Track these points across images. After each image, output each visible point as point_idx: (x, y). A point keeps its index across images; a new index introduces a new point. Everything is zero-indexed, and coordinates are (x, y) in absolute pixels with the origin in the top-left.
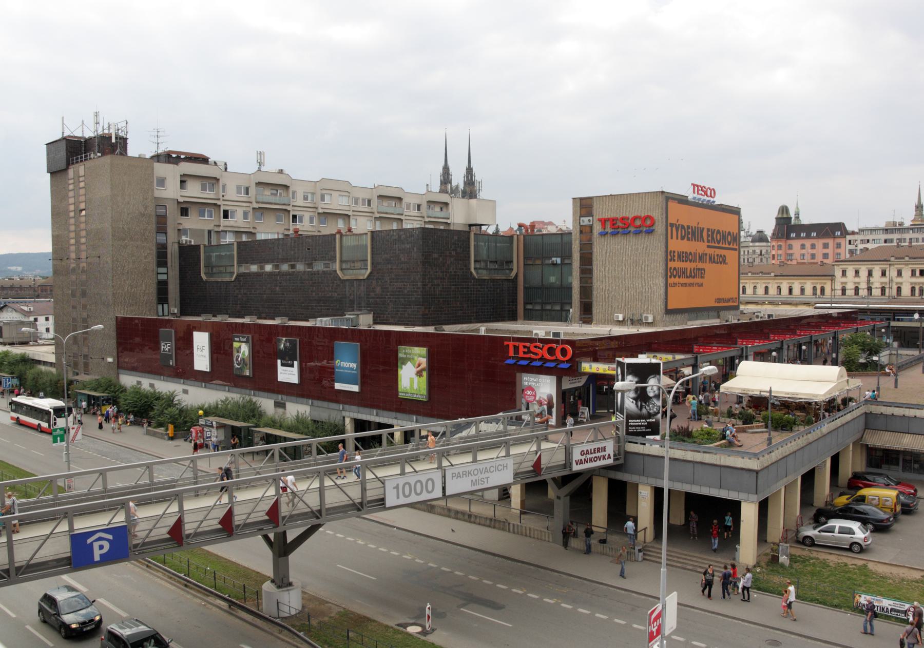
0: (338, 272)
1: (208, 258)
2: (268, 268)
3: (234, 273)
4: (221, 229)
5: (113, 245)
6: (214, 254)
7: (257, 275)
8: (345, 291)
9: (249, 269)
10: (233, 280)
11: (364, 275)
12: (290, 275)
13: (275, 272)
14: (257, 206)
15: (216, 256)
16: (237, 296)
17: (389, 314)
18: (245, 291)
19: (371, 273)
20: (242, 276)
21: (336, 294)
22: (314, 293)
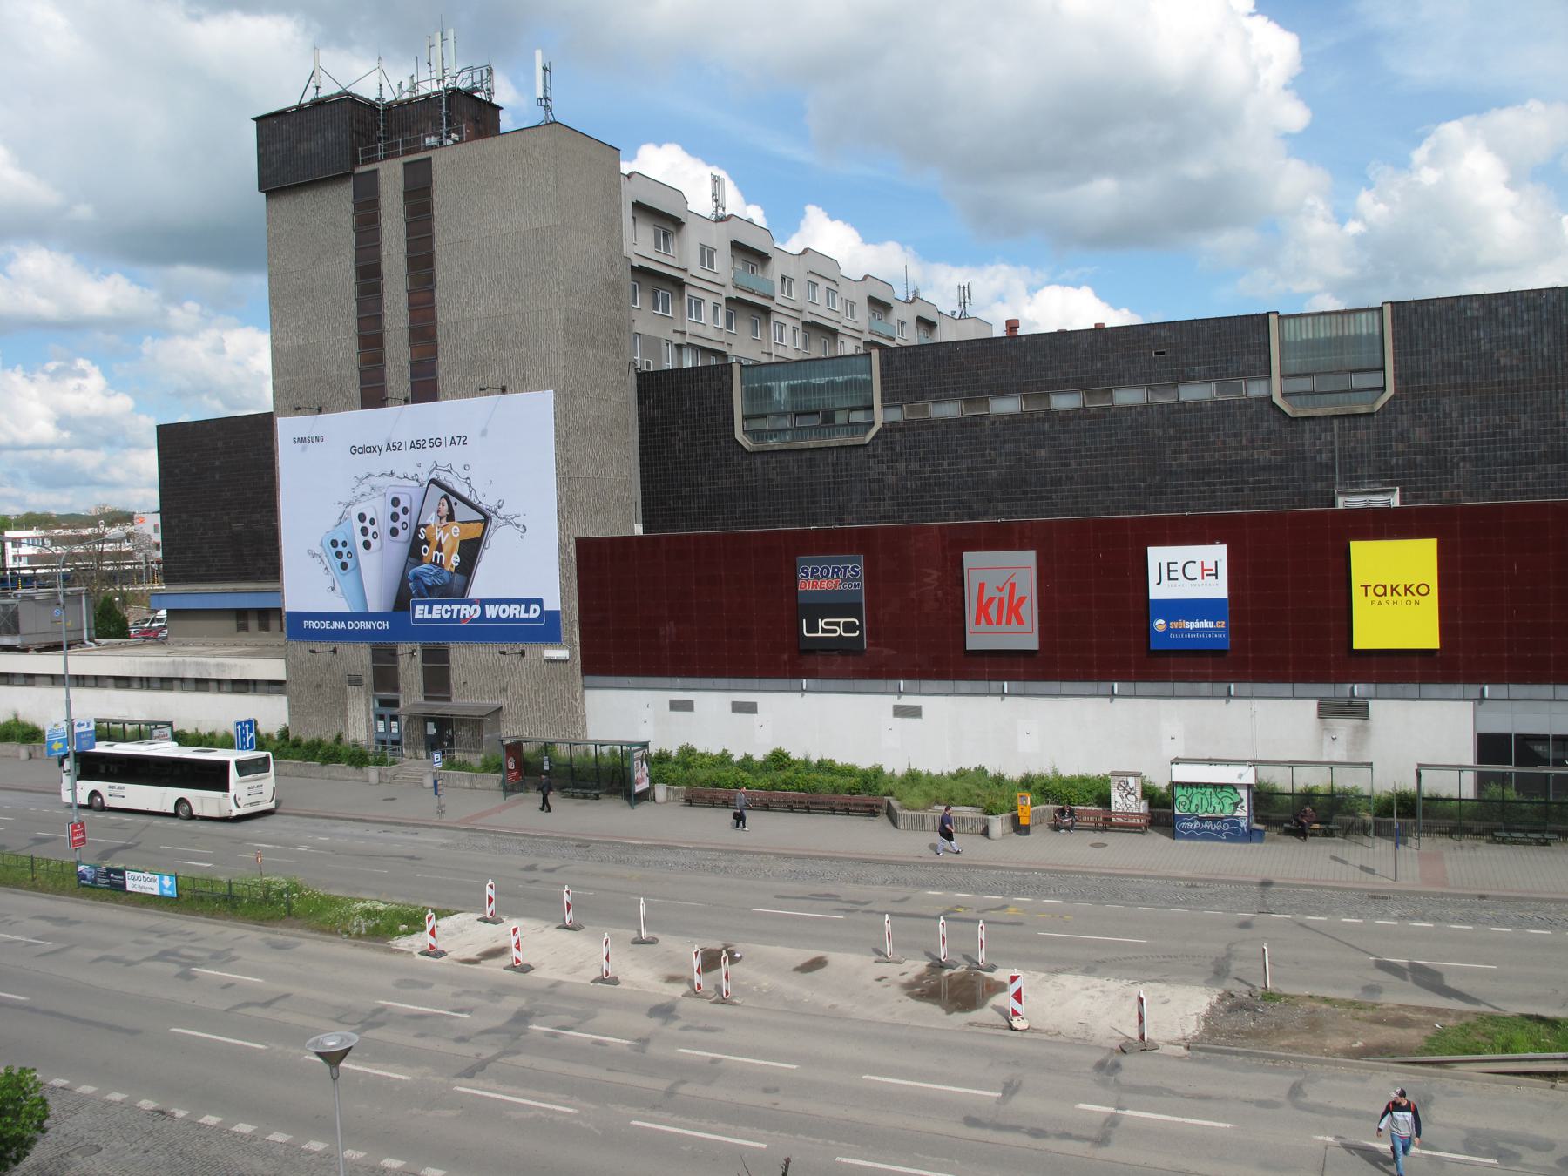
0: (1277, 400)
1: (759, 395)
2: (1006, 406)
3: (872, 424)
4: (688, 340)
5: (565, 353)
6: (783, 384)
7: (964, 425)
8: (1303, 445)
9: (926, 410)
10: (866, 443)
11: (1374, 402)
12: (1094, 416)
13: (1031, 414)
14: (734, 294)
15: (791, 388)
16: (879, 481)
17: (1458, 487)
18: (914, 466)
19: (1394, 397)
20: (900, 430)
21: (1267, 453)
22: (1074, 467)
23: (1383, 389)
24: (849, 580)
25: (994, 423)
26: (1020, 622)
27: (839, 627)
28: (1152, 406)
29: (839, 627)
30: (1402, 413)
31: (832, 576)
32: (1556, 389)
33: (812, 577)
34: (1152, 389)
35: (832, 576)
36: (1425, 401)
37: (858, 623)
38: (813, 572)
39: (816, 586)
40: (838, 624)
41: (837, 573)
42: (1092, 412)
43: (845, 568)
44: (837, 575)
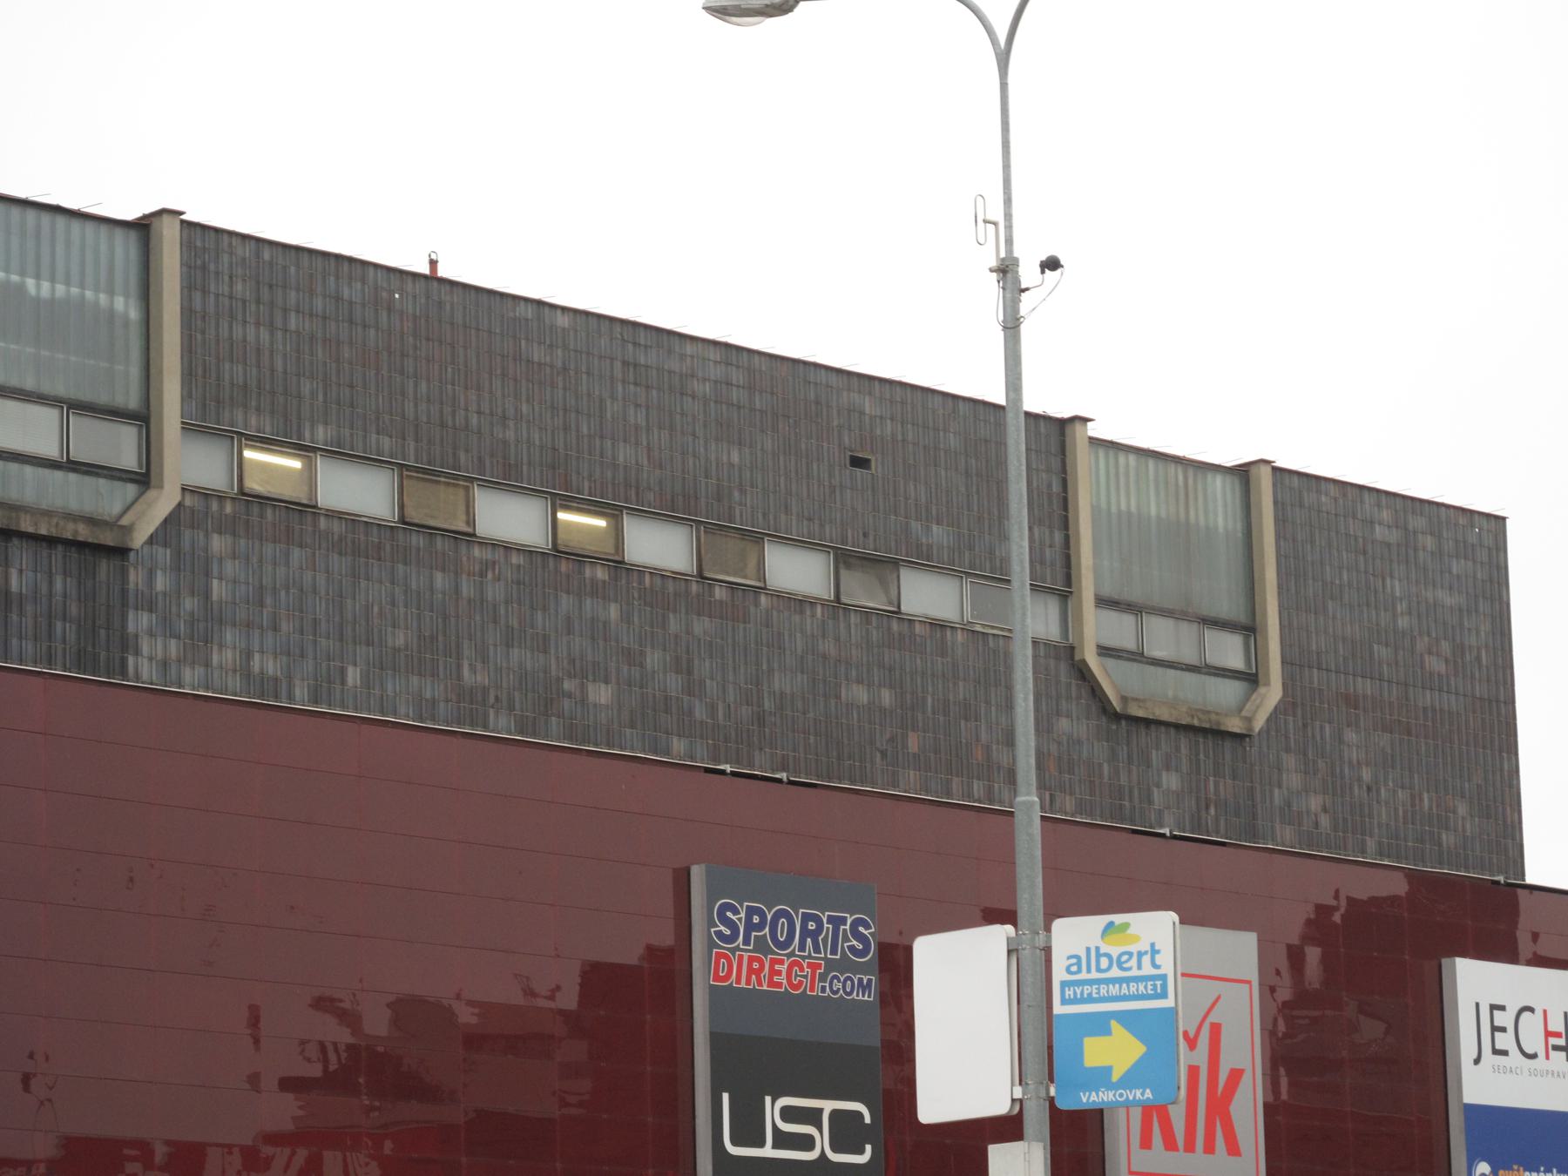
23: (1252, 678)
24: (844, 965)
25: (487, 566)
26: (1233, 1149)
27: (820, 1128)
28: (847, 609)
29: (820, 1128)
30: (1288, 750)
31: (802, 947)
32: (1501, 751)
33: (747, 942)
34: (845, 563)
35: (802, 947)
36: (1322, 728)
37: (868, 1120)
38: (750, 927)
39: (758, 972)
40: (813, 1117)
41: (815, 935)
42: (719, 593)
43: (837, 922)
44: (817, 950)
